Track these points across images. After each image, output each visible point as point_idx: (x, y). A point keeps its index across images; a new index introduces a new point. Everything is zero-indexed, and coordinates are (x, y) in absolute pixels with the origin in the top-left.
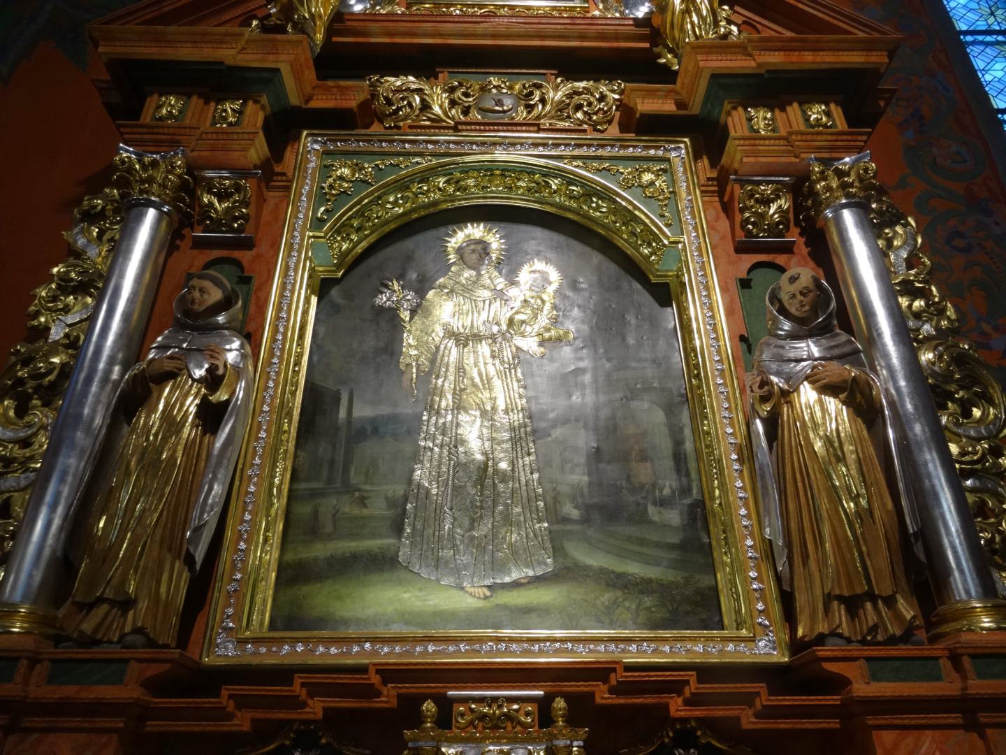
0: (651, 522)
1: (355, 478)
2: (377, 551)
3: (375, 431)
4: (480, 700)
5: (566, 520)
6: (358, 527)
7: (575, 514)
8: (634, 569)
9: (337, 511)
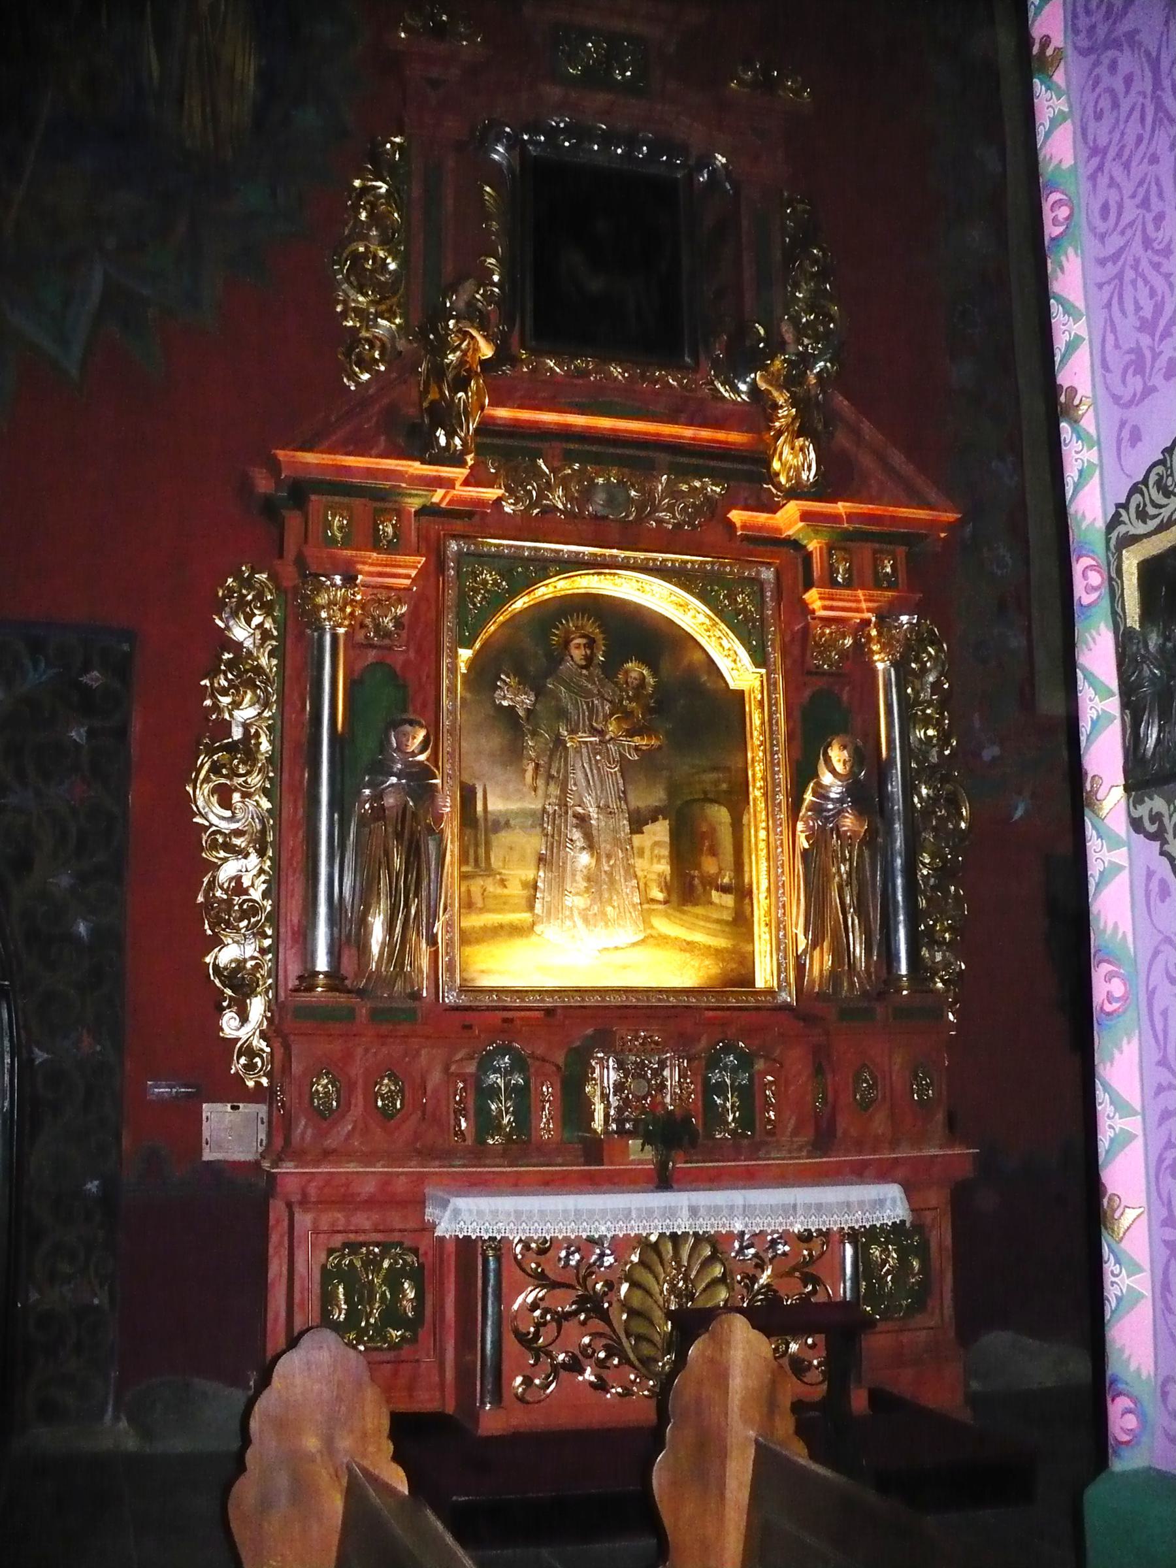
0: (711, 903)
1: (495, 862)
2: (517, 922)
3: (507, 824)
4: (443, 992)
5: (653, 901)
6: (503, 904)
7: (660, 896)
8: (699, 937)
9: (485, 890)
